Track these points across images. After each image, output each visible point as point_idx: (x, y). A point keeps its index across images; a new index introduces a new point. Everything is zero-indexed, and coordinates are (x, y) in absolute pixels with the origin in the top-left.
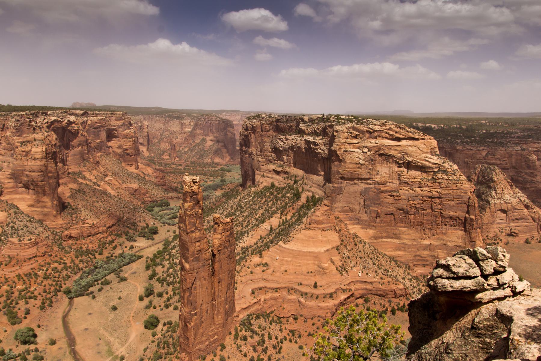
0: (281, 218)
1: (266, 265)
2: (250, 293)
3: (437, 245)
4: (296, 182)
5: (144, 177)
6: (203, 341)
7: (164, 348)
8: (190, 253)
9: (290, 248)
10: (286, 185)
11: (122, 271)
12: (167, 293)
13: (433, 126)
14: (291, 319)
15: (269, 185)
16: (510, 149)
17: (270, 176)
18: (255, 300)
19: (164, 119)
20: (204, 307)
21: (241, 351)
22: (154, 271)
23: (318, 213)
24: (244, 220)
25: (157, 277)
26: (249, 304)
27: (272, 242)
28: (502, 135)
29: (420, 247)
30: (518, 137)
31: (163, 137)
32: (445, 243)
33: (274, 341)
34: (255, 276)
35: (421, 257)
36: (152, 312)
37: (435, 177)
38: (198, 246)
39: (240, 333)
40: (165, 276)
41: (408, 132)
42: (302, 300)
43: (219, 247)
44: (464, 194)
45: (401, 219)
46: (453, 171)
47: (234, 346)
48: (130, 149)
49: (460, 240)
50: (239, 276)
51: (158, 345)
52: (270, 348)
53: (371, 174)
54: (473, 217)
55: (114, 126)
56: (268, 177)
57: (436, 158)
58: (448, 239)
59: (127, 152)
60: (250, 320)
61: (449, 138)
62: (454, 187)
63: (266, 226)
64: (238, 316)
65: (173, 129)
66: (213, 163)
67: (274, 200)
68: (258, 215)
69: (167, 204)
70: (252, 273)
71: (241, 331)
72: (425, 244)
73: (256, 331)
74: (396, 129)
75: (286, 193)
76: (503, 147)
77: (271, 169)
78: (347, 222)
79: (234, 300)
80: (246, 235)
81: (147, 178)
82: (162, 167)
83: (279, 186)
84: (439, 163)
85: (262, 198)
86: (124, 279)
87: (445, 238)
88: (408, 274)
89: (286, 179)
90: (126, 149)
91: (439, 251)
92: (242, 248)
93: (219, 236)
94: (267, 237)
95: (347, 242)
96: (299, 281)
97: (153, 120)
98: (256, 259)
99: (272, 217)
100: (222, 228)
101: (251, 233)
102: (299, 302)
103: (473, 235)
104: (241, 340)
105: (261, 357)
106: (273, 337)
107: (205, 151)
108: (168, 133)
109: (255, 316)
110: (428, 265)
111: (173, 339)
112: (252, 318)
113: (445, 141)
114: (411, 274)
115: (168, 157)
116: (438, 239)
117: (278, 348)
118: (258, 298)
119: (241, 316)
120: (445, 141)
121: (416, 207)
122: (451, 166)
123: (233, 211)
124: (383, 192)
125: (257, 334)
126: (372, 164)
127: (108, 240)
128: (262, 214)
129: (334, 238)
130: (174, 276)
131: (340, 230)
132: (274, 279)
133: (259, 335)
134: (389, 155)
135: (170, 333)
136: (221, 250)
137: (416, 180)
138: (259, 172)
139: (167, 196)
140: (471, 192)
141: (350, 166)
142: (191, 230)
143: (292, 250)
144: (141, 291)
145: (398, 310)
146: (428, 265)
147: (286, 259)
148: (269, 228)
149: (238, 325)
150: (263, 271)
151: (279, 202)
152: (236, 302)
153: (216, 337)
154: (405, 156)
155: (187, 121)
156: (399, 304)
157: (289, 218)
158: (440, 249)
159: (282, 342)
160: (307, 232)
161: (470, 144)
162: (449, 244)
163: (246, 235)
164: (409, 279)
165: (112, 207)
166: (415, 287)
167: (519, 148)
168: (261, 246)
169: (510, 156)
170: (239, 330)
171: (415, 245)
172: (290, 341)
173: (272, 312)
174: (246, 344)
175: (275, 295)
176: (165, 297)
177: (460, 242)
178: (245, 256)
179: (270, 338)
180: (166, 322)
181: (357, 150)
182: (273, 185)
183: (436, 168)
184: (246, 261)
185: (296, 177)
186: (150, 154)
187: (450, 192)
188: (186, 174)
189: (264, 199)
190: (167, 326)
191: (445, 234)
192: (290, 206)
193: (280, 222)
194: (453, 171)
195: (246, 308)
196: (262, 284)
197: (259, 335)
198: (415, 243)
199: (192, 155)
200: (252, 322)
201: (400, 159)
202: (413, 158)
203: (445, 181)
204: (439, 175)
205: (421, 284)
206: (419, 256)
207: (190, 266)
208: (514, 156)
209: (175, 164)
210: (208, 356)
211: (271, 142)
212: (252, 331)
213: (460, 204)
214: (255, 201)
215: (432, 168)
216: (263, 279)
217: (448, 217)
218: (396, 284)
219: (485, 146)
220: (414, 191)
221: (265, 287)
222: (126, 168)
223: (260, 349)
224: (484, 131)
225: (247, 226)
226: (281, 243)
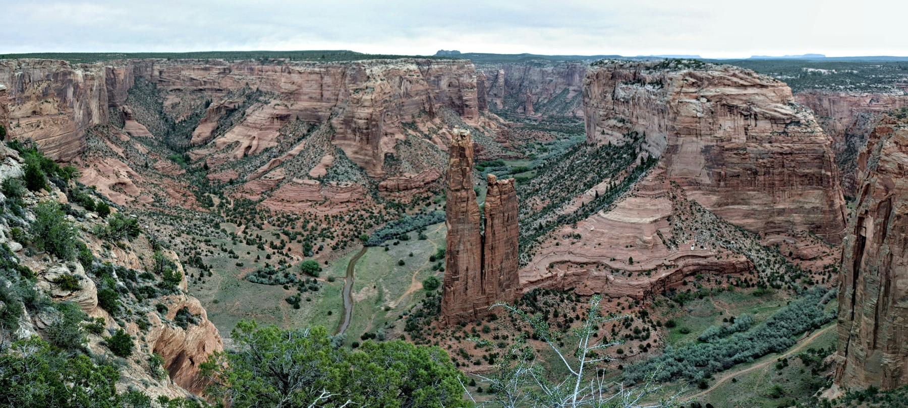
4: (636, 139)
17: (610, 132)
23: (650, 178)
27: (592, 211)
42: (611, 277)
53: (711, 130)
63: (591, 192)
66: (575, 117)
74: (741, 75)
77: (611, 125)
78: (685, 188)
95: (684, 211)
96: (611, 255)
98: (568, 229)
102: (607, 279)
115: (522, 111)
124: (727, 150)
126: (713, 118)
128: (593, 178)
129: (665, 206)
131: (674, 197)
132: (583, 252)
134: (733, 106)
141: (687, 119)
148: (594, 194)
151: (613, 164)
157: (617, 182)
159: (571, 321)
160: (633, 200)
173: (572, 289)
175: (580, 270)
181: (694, 101)
185: (637, 134)
201: (746, 111)
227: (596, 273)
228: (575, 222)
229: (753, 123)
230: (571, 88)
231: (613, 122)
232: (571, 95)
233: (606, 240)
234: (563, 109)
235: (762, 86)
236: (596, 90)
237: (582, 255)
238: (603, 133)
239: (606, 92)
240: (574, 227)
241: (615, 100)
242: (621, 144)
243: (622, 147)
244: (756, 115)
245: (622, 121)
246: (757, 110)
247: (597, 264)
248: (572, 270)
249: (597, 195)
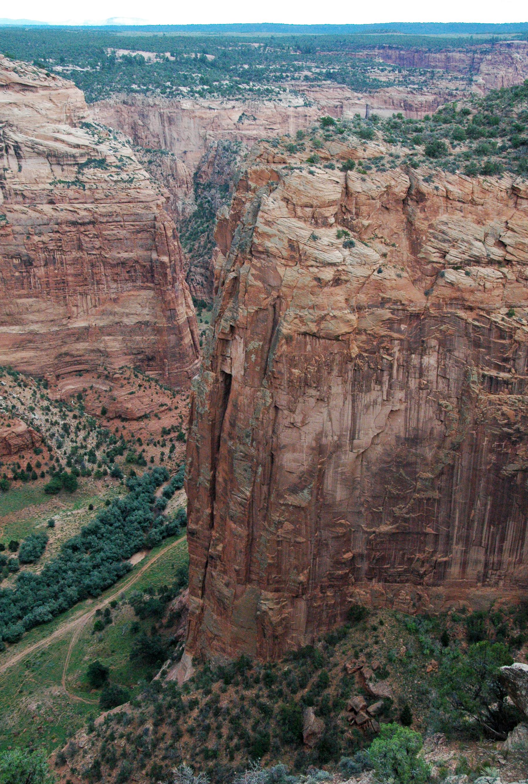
3: (103, 327)
13: (146, 55)
16: (284, 104)
28: (278, 74)
29: (69, 335)
30: (307, 78)
32: (117, 320)
35: (72, 356)
37: (80, 176)
41: (6, 69)
44: (144, 211)
45: (18, 278)
46: (121, 160)
49: (146, 311)
54: (165, 259)
57: (80, 132)
58: (123, 310)
61: (169, 84)
62: (122, 195)
72: (79, 328)
76: (270, 100)
84: (87, 143)
87: (117, 309)
88: (42, 397)
91: (107, 338)
103: (170, 296)
110: (87, 371)
113: (159, 90)
114: (50, 396)
116: (103, 313)
120: (159, 90)
121: (46, 249)
122: (116, 150)
137: (41, 186)
140: (158, 206)
145: (15, 479)
146: (87, 371)
154: (7, 130)
156: (19, 467)
158: (109, 335)
161: (208, 96)
162: (126, 320)
164: (43, 409)
166: (57, 423)
167: (300, 101)
169: (285, 119)
171: (57, 333)
177: (145, 314)
183: (82, 155)
187: (116, 208)
191: (115, 301)
194: (121, 160)
198: (57, 329)
202: (26, 134)
203: (104, 185)
204: (89, 172)
205: (71, 414)
206: (67, 354)
208: (291, 120)
213: (139, 232)
215: (74, 156)
217: (118, 264)
218: (9, 426)
219: (237, 100)
220: (39, 212)
224: (246, 67)
229: (13, 163)
235: (25, 88)
244: (17, 148)
246: (19, 137)
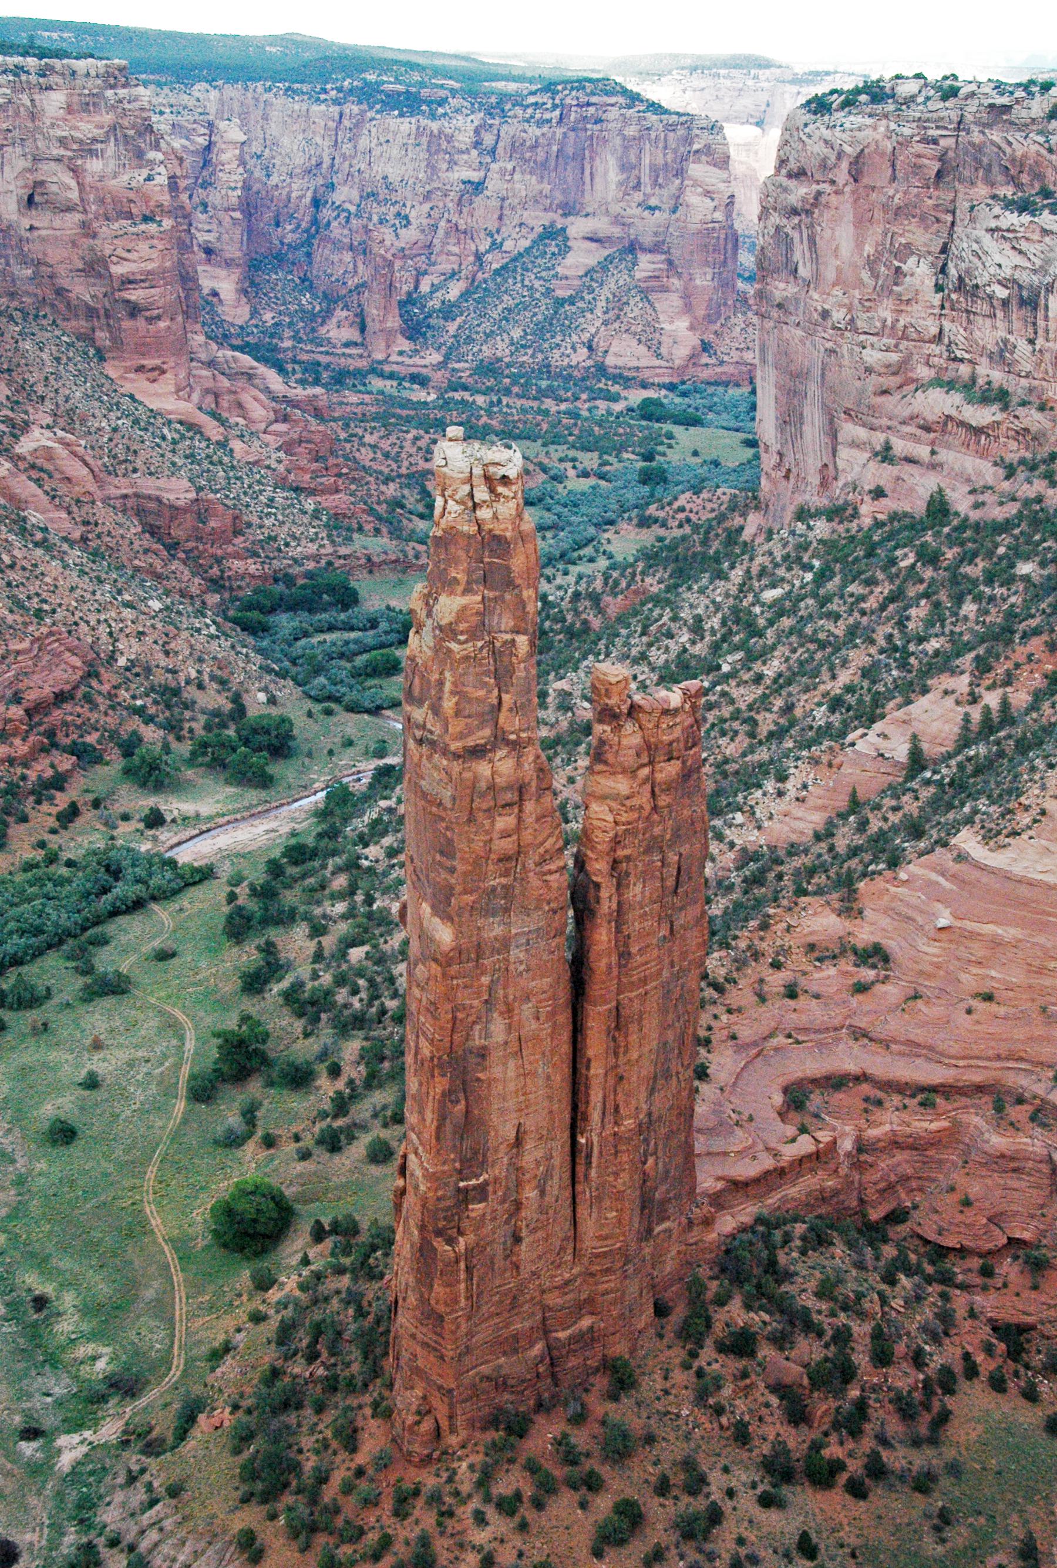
0: (974, 699)
1: (875, 955)
2: (778, 1099)
5: (223, 444)
6: (516, 1337)
7: (312, 1357)
8: (461, 867)
9: (1018, 870)
10: (1012, 509)
11: (103, 941)
12: (335, 1071)
14: (1008, 1268)
15: (918, 507)
17: (923, 452)
18: (805, 1145)
19: (335, 110)
20: (532, 1154)
21: (719, 1411)
22: (269, 949)
24: (763, 703)
25: (285, 984)
26: (768, 1163)
27: (916, 831)
31: (326, 213)
33: (903, 1378)
34: (809, 1011)
36: (250, 1165)
38: (505, 835)
39: (720, 1317)
40: (327, 979)
43: (616, 842)
47: (679, 1377)
48: (146, 280)
50: (719, 1010)
51: (285, 1334)
52: (883, 1417)
55: (62, 142)
56: (910, 460)
59: (135, 295)
60: (771, 1248)
63: (886, 741)
64: (708, 1222)
65: (380, 169)
66: (601, 369)
67: (943, 596)
68: (845, 677)
69: (348, 599)
70: (791, 992)
71: (721, 1301)
73: (806, 1311)
75: (1017, 554)
79: (689, 1129)
80: (770, 785)
81: (237, 445)
82: (318, 390)
83: (975, 515)
85: (871, 582)
86: (114, 987)
89: (1021, 475)
90: (128, 282)
92: (747, 856)
93: (622, 785)
94: (888, 802)
97: (274, 115)
98: (820, 921)
99: (925, 691)
100: (636, 740)
101: (799, 774)
104: (722, 1348)
105: (826, 1453)
106: (900, 1348)
107: (560, 302)
108: (355, 195)
109: (800, 1228)
111: (361, 1313)
112: (787, 1239)
115: (349, 333)
117: (925, 1418)
118: (825, 1136)
119: (726, 1224)
123: (700, 649)
125: (810, 1328)
127: (32, 775)
130: (371, 982)
132: (918, 1034)
133: (820, 1334)
135: (346, 1280)
136: (628, 858)
138: (862, 433)
139: (343, 551)
142: (470, 742)
143: (1031, 883)
144: (196, 1050)
147: (989, 929)
148: (901, 751)
149: (704, 1272)
150: (861, 988)
151: (969, 608)
152: (699, 1147)
153: (586, 1322)
155: (460, 121)
157: (1020, 698)
159: (947, 1382)
163: (770, 785)
165: (55, 600)
168: (854, 851)
170: (709, 1295)
172: (998, 1384)
173: (897, 1216)
174: (745, 1375)
176: (327, 1088)
178: (759, 903)
179: (882, 1358)
180: (326, 1221)
182: (939, 509)
184: (764, 926)
186: (254, 313)
188: (453, 431)
189: (885, 589)
190: (329, 1243)
192: (1036, 632)
193: (967, 719)
195: (757, 1181)
196: (849, 1058)
197: (820, 1334)
199: (487, 326)
200: (782, 1258)
207: (458, 934)
209: (391, 376)
210: (540, 1419)
211: (944, 250)
212: (781, 1306)
214: (828, 599)
216: (860, 1034)
221: (862, 1078)
222: (127, 388)
223: (823, 1406)
225: (777, 735)
226: (967, 840)
227: (998, 1141)
228: (847, 884)
230: (577, 227)
231: (938, 403)
232: (581, 258)
233: (1017, 977)
234: (542, 330)
236: (842, 239)
237: (914, 1048)
238: (885, 455)
239: (906, 252)
240: (850, 909)
241: (960, 291)
242: (998, 513)
243: (1005, 527)
245: (1001, 397)
247: (999, 1099)
248: (888, 1123)
249: (917, 762)
